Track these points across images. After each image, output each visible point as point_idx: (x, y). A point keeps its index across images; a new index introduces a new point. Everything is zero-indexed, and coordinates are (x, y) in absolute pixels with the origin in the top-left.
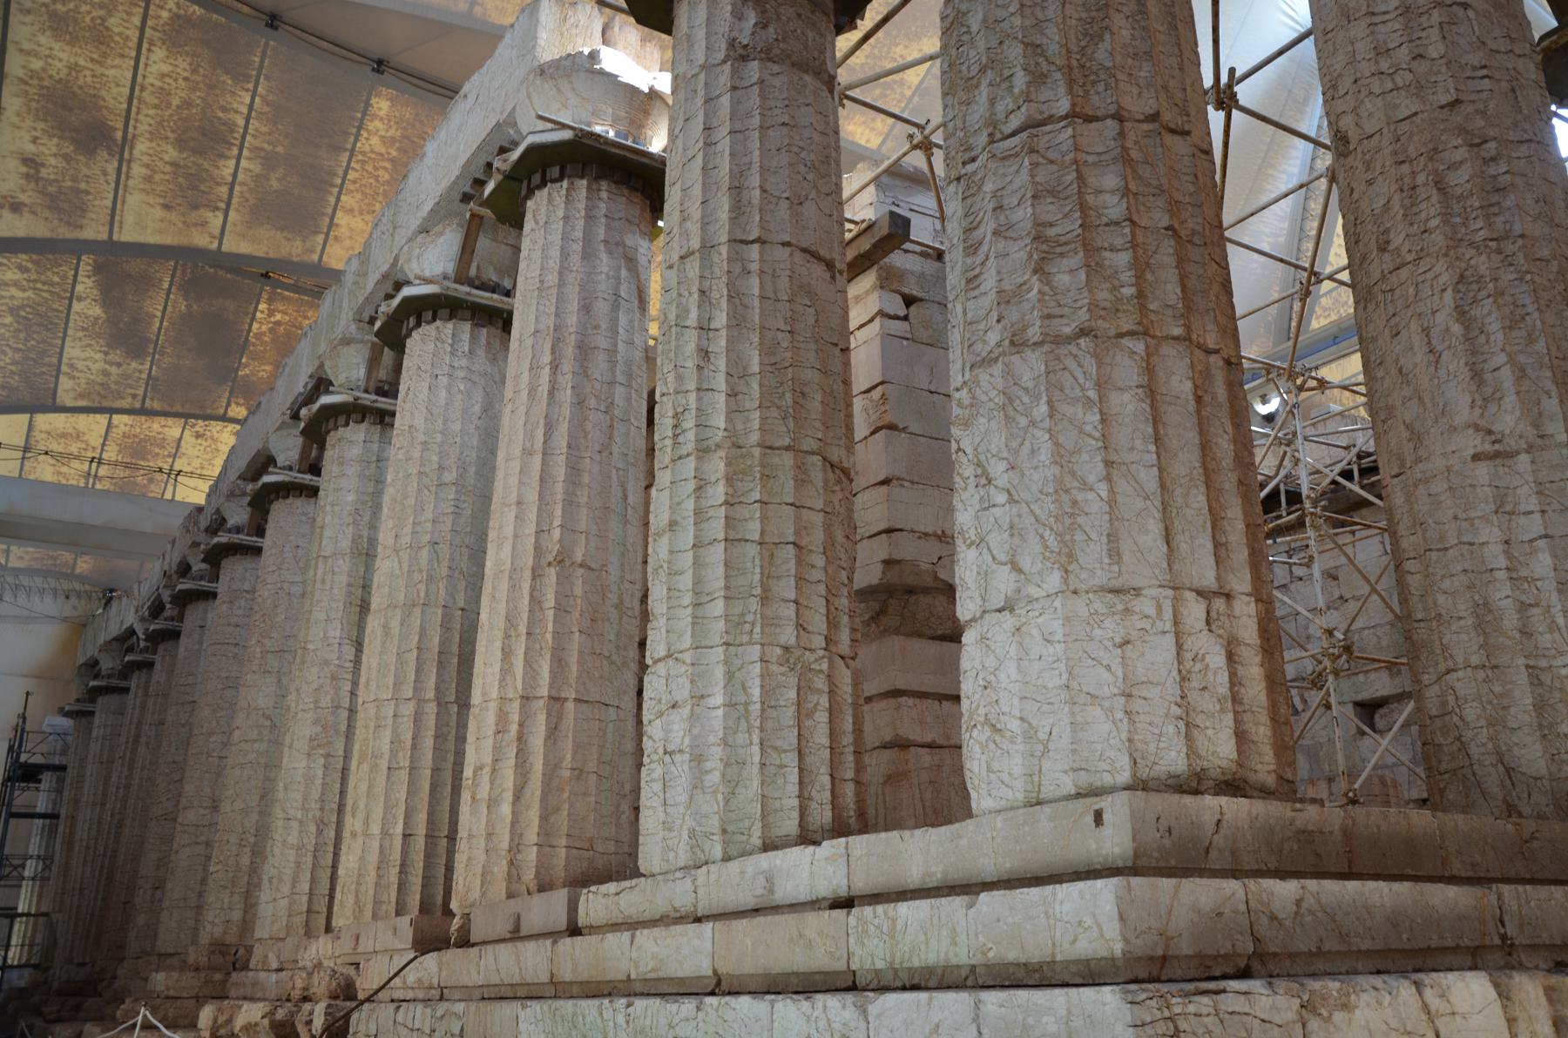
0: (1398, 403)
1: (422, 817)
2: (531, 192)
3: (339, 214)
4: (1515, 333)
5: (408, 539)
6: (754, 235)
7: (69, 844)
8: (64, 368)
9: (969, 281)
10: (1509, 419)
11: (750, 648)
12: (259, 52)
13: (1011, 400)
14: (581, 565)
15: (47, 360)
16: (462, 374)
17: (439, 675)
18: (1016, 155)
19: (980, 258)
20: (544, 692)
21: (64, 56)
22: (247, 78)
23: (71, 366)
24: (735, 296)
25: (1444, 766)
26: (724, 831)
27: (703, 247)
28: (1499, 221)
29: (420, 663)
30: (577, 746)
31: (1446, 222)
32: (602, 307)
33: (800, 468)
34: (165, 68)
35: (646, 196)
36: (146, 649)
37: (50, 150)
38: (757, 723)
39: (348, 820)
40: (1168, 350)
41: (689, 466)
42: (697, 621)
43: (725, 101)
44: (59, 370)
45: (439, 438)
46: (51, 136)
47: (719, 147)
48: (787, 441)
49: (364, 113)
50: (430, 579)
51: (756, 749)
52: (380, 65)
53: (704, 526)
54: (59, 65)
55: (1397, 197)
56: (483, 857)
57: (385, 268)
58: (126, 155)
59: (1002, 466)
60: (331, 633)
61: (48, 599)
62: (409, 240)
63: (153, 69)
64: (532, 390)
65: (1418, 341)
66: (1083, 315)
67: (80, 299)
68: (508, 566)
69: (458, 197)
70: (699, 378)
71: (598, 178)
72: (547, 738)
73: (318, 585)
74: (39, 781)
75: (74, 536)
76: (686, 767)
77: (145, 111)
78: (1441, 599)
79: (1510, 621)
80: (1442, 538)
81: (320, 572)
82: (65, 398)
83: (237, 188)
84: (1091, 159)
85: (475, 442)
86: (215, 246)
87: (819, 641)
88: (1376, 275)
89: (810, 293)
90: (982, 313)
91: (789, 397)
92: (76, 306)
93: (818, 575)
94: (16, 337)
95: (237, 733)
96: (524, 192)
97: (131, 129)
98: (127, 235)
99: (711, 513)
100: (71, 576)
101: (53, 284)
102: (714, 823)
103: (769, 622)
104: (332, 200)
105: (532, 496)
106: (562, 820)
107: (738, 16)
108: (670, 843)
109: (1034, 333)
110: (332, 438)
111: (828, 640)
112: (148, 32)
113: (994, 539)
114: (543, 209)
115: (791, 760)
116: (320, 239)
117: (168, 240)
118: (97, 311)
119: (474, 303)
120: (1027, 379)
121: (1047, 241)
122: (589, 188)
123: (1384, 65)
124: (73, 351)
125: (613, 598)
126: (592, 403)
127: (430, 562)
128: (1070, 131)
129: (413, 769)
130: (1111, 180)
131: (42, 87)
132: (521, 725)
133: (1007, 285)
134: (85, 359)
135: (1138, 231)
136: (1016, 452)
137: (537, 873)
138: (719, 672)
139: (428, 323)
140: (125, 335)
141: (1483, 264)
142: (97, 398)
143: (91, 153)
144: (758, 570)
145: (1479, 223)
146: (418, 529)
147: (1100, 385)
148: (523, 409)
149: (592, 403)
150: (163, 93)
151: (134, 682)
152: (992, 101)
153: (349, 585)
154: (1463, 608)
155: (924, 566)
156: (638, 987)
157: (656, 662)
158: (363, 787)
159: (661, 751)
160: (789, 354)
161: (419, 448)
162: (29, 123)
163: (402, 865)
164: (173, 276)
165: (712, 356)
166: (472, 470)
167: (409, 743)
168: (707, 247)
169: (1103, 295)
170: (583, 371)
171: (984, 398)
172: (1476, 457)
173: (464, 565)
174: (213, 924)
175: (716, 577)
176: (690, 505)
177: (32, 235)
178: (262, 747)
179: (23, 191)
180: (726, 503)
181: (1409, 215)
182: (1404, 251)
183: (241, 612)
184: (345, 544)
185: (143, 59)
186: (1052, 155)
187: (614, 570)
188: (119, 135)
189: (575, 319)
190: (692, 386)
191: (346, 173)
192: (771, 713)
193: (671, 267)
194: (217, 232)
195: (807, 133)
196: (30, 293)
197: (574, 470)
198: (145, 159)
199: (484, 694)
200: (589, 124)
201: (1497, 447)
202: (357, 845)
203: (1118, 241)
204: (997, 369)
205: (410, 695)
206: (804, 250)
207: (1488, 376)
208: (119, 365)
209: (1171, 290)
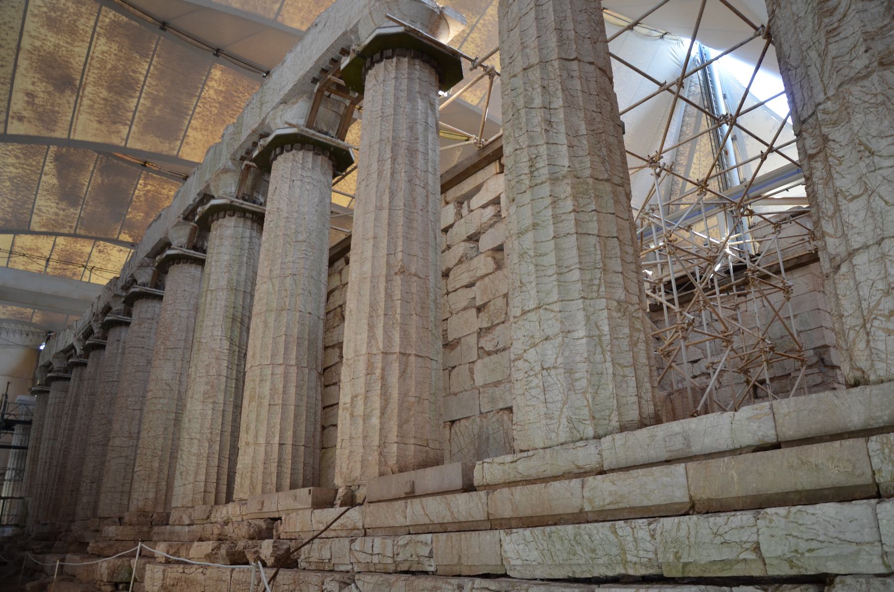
1: (290, 434)
2: (372, 65)
3: (190, 130)
7: (34, 461)
8: (35, 211)
11: (598, 301)
12: (154, 42)
14: (415, 275)
15: (26, 206)
16: (307, 180)
17: (298, 351)
20: (397, 349)
21: (52, 40)
22: (147, 56)
23: (39, 210)
26: (594, 418)
29: (287, 344)
32: (420, 128)
34: (105, 48)
36: (81, 356)
37: (40, 89)
38: (609, 348)
39: (243, 435)
41: (546, 189)
42: (561, 284)
44: (32, 212)
45: (295, 215)
46: (42, 82)
48: (606, 176)
49: (207, 77)
51: (609, 365)
52: (218, 52)
53: (560, 225)
54: (49, 44)
56: (362, 450)
58: (81, 94)
60: (215, 333)
61: (17, 336)
62: (274, 108)
63: (99, 48)
64: (380, 173)
67: (46, 174)
71: (414, 58)
72: (400, 377)
73: (207, 306)
74: (13, 430)
75: (34, 299)
77: (92, 71)
81: (208, 299)
82: (35, 227)
83: (137, 114)
86: (123, 144)
91: (604, 149)
92: (44, 178)
94: (11, 193)
95: (149, 395)
96: (368, 64)
97: (84, 80)
98: (78, 136)
100: (30, 324)
101: (32, 166)
103: (609, 285)
104: (186, 122)
105: (383, 233)
108: (552, 427)
110: (214, 226)
112: (98, 29)
116: (178, 143)
117: (99, 140)
118: (55, 181)
119: (316, 140)
124: (40, 202)
129: (283, 405)
131: (39, 56)
132: (383, 369)
133: (869, 28)
134: (46, 207)
137: (398, 460)
138: (580, 316)
139: (288, 151)
140: (68, 194)
142: (51, 227)
143: (62, 92)
144: (599, 252)
146: (284, 266)
150: (103, 62)
151: (74, 374)
153: (226, 306)
156: (591, 517)
157: (524, 313)
158: (253, 416)
159: (538, 368)
160: (601, 126)
161: (283, 220)
162: (31, 74)
163: (279, 462)
164: (96, 164)
165: (554, 124)
166: (314, 234)
167: (281, 390)
168: (544, 63)
170: (412, 164)
174: (138, 500)
175: (572, 256)
176: (549, 212)
177: (28, 133)
178: (166, 401)
179: (25, 110)
180: (574, 211)
183: (145, 330)
184: (223, 283)
185: (94, 43)
188: (78, 82)
189: (404, 133)
190: (542, 141)
191: (195, 108)
193: (515, 76)
194: (125, 137)
196: (20, 170)
197: (409, 220)
198: (90, 96)
199: (356, 351)
202: (250, 450)
206: (600, 69)
208: (64, 210)
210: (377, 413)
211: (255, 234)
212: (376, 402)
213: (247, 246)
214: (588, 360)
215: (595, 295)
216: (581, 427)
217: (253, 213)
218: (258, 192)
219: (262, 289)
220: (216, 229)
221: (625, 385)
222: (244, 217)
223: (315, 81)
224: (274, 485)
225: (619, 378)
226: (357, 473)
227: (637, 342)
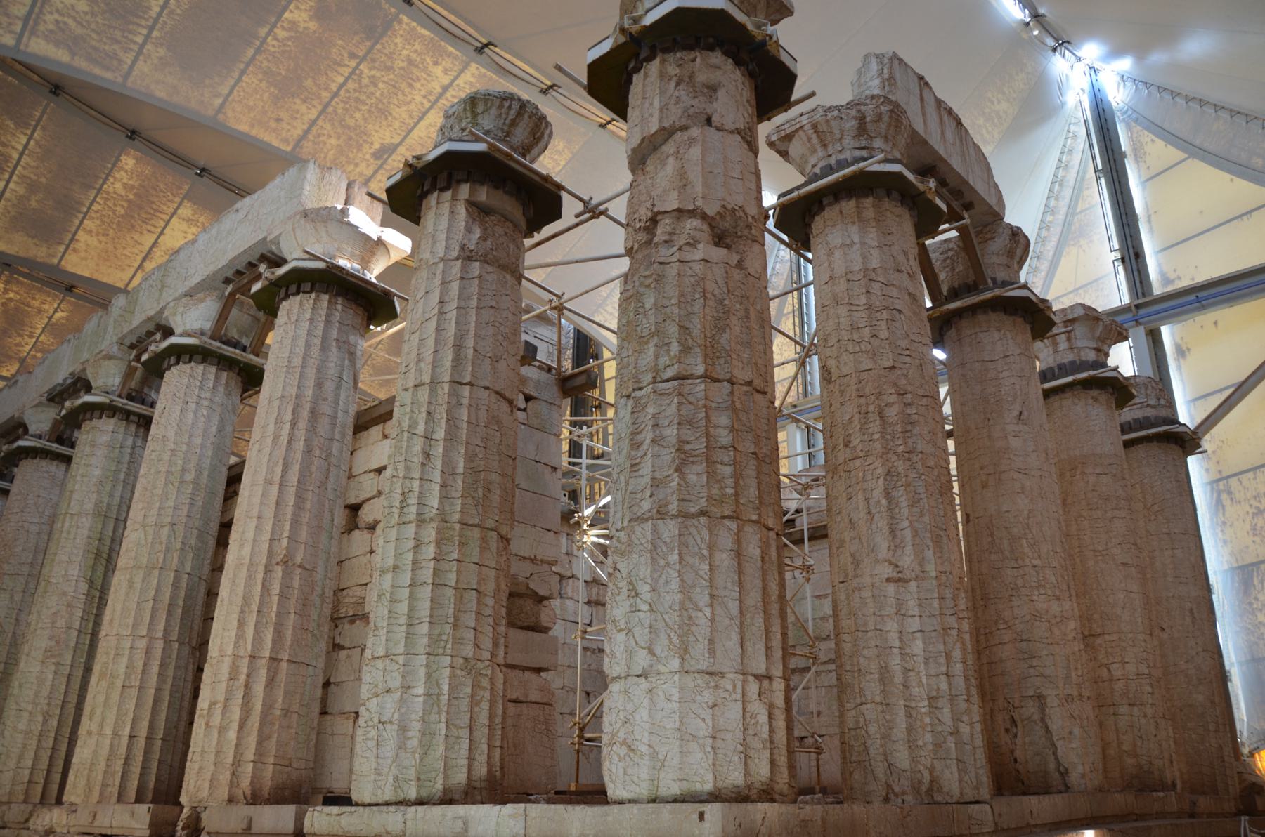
0: (847, 539)
2: (287, 296)
4: (915, 509)
5: (154, 519)
6: (467, 379)
9: (632, 466)
10: (907, 560)
11: (443, 658)
13: (655, 548)
14: (299, 566)
16: (206, 403)
18: (669, 394)
19: (640, 453)
24: (451, 419)
25: (853, 758)
26: (419, 779)
27: (432, 382)
28: (910, 441)
30: (286, 693)
31: (883, 437)
32: (329, 386)
33: (484, 539)
35: (366, 310)
40: (749, 529)
41: (411, 530)
43: (455, 286)
45: (184, 448)
47: (448, 316)
48: (476, 521)
50: (168, 549)
51: (443, 726)
55: (857, 416)
56: (212, 767)
57: (152, 313)
59: (647, 588)
64: (276, 438)
65: (862, 504)
66: (703, 503)
68: (247, 561)
69: (222, 279)
70: (423, 472)
71: (338, 294)
72: (266, 686)
76: (394, 734)
78: (862, 660)
79: (898, 678)
80: (865, 624)
84: (714, 405)
85: (210, 453)
87: (487, 655)
88: (841, 460)
89: (498, 422)
90: (640, 488)
93: (488, 611)
99: (423, 564)
102: (412, 773)
103: (457, 641)
105: (269, 513)
106: (272, 745)
107: (469, 230)
109: (673, 508)
111: (492, 654)
113: (637, 631)
114: (296, 311)
115: (465, 734)
120: (666, 536)
121: (685, 452)
122: (329, 301)
123: (855, 337)
125: (318, 590)
126: (317, 452)
127: (169, 537)
128: (703, 386)
130: (724, 420)
132: (248, 676)
133: (658, 475)
135: (738, 454)
136: (656, 581)
137: (252, 782)
138: (422, 672)
141: (901, 466)
145: (900, 442)
147: (710, 548)
148: (267, 451)
149: (317, 452)
152: (657, 356)
154: (874, 667)
155: (521, 579)
157: (374, 658)
159: (376, 720)
161: (169, 453)
166: (206, 473)
167: (140, 669)
168: (434, 383)
169: (715, 491)
171: (637, 542)
172: (888, 580)
173: (193, 542)
176: (410, 556)
180: (435, 559)
181: (863, 428)
182: (858, 449)
186: (691, 399)
187: (320, 570)
190: (417, 475)
192: (455, 702)
193: (406, 390)
195: (505, 314)
197: (300, 498)
199: (221, 651)
200: (334, 257)
203: (726, 459)
204: (648, 526)
205: (144, 633)
206: (497, 393)
207: (898, 533)
209: (752, 492)
210: (235, 726)
211: (139, 442)
212: (236, 714)
213: (127, 458)
214: (423, 719)
215: (441, 651)
216: (406, 787)
217: (139, 416)
218: (150, 387)
219: (133, 537)
220: (88, 432)
221: (457, 747)
222: (127, 419)
223: (227, 281)
224: (117, 787)
225: (451, 740)
226: (204, 793)
227: (481, 700)
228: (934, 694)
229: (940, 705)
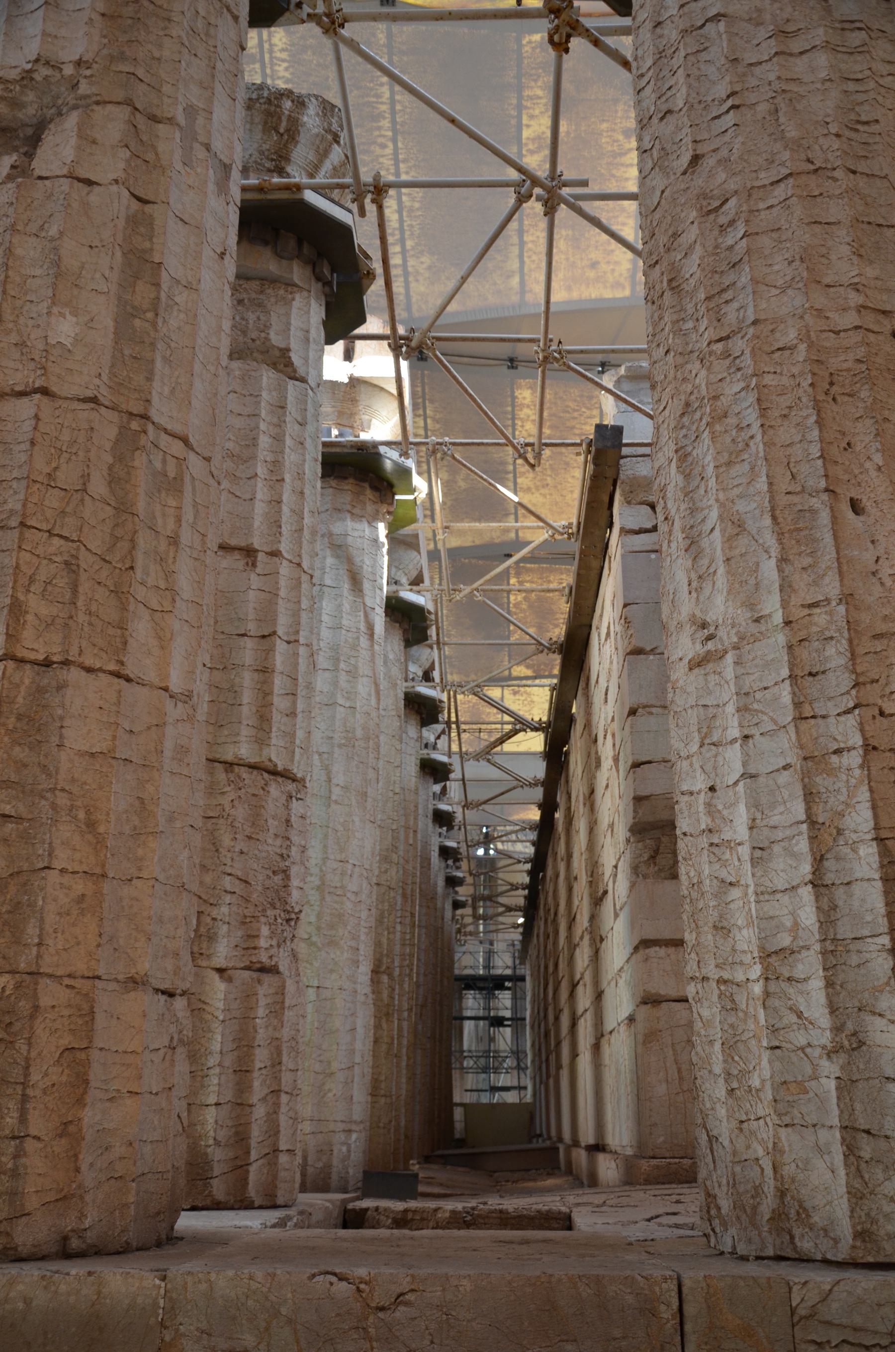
201: (710, 645)
228: (785, 940)
229: (800, 971)
